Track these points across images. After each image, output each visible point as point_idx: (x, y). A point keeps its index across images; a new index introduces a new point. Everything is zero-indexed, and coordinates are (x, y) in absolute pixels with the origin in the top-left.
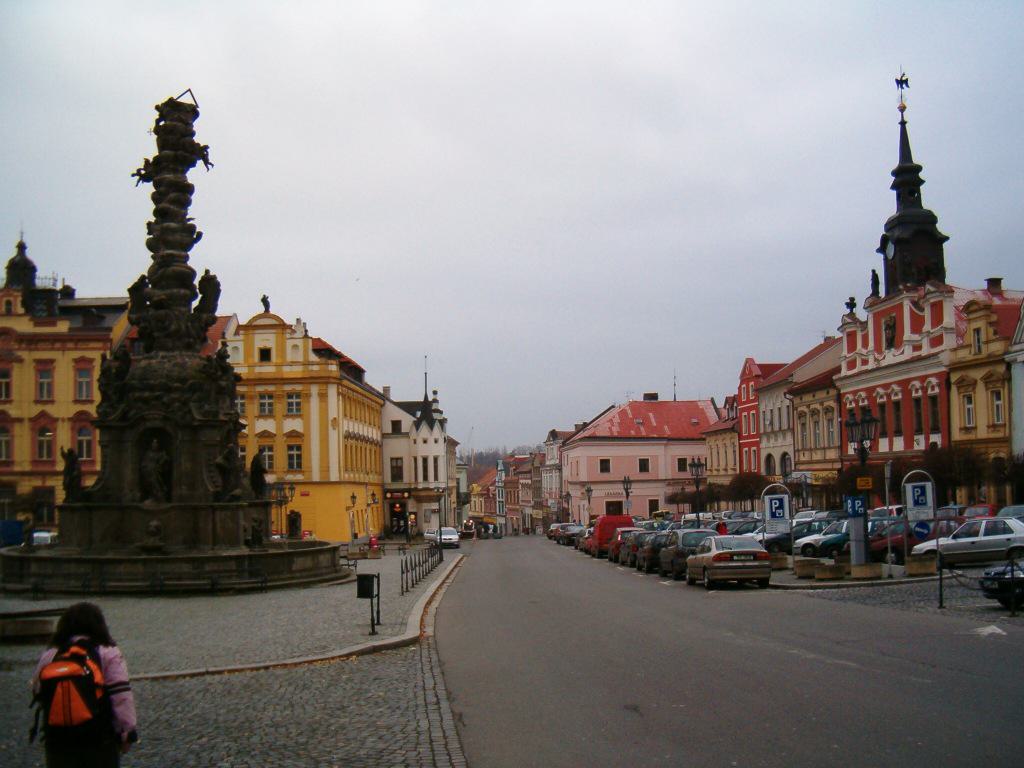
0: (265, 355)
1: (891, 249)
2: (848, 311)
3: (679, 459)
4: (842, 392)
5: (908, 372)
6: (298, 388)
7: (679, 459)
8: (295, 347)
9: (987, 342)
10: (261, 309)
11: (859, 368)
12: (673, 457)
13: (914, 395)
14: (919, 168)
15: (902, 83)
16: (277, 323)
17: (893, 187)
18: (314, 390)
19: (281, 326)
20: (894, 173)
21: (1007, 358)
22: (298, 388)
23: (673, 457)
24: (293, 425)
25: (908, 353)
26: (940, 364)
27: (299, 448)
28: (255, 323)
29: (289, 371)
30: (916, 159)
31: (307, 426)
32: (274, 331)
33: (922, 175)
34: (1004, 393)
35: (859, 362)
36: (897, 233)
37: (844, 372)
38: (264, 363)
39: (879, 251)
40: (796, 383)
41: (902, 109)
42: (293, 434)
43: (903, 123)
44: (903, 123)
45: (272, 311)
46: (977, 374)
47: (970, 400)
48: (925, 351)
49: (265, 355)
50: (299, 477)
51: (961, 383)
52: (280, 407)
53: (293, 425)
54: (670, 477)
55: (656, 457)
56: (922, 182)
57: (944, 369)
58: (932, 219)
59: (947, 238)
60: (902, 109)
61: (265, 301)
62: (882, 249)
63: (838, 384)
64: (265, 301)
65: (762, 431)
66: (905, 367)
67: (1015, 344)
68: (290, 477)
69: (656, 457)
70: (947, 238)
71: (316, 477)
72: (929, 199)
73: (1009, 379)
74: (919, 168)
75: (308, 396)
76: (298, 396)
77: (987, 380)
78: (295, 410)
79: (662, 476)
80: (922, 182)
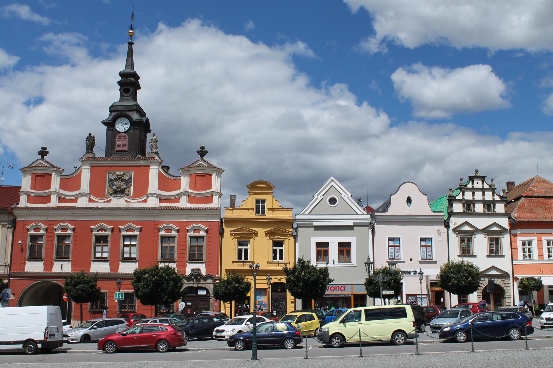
1: (122, 126)
2: (40, 157)
4: (19, 219)
5: (156, 216)
11: (54, 202)
20: (121, 74)
25: (153, 202)
35: (54, 198)
37: (23, 202)
39: (105, 123)
48: (183, 203)
62: (110, 124)
63: (16, 212)
66: (155, 212)
67: (303, 214)
73: (295, 238)
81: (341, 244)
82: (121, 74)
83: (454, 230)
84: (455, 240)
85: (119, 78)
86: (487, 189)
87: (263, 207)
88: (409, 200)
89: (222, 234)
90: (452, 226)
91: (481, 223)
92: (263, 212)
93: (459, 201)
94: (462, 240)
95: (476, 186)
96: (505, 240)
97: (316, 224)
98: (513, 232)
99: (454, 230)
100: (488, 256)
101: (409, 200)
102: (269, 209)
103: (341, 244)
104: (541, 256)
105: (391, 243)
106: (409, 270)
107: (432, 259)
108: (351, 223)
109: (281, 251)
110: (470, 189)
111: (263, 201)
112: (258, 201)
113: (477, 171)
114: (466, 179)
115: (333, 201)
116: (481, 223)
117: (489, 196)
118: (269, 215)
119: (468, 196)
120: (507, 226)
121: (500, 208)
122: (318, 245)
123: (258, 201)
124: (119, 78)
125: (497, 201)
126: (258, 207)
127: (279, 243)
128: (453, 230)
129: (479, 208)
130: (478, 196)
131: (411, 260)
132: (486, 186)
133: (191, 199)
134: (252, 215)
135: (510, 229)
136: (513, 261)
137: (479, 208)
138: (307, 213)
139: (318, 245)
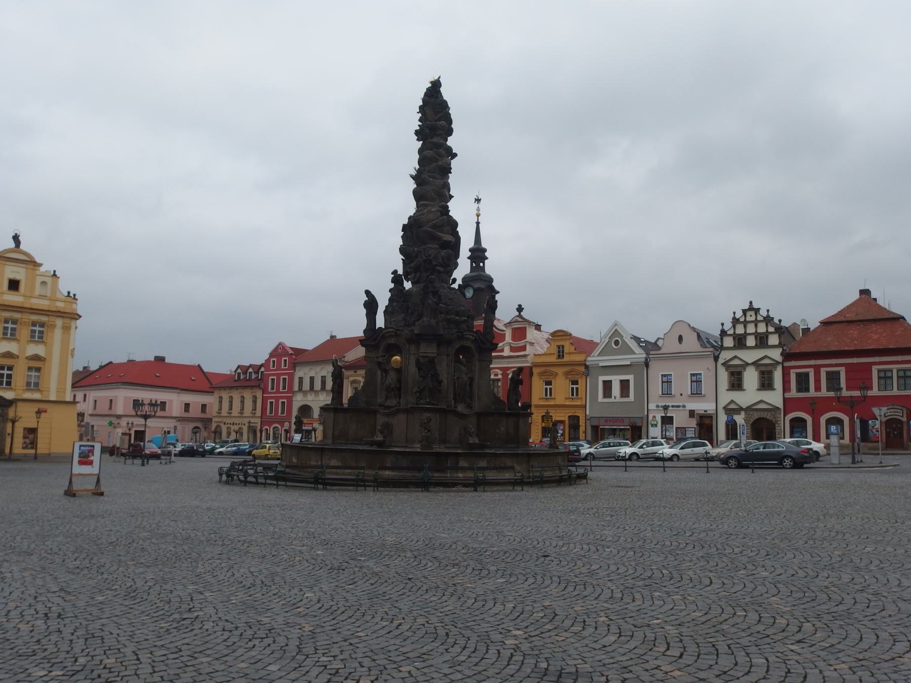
3: (185, 404)
6: (44, 319)
7: (185, 404)
9: (570, 353)
10: (12, 245)
13: (492, 377)
14: (485, 250)
15: (478, 200)
16: (28, 259)
17: (468, 258)
18: (59, 322)
19: (32, 263)
20: (471, 250)
21: (587, 363)
22: (44, 319)
24: (39, 350)
26: (527, 362)
27: (38, 370)
28: (7, 255)
29: (36, 303)
30: (484, 245)
31: (50, 352)
33: (486, 254)
34: (581, 382)
36: (477, 285)
38: (11, 292)
40: (346, 362)
41: (478, 215)
42: (36, 358)
43: (478, 223)
44: (478, 223)
45: (23, 247)
46: (560, 371)
47: (549, 383)
49: (14, 285)
50: (37, 396)
51: (541, 374)
52: (24, 333)
53: (39, 350)
54: (179, 416)
55: (171, 401)
56: (487, 258)
57: (529, 365)
58: (490, 280)
59: (498, 292)
60: (478, 215)
61: (16, 238)
64: (16, 238)
65: (296, 388)
67: (593, 356)
68: (28, 395)
69: (171, 401)
70: (498, 292)
71: (53, 398)
72: (490, 268)
74: (485, 250)
76: (42, 325)
77: (567, 374)
78: (39, 337)
79: (174, 415)
80: (487, 258)
81: (621, 381)
82: (471, 250)
83: (723, 364)
84: (723, 376)
85: (470, 253)
86: (761, 321)
87: (563, 352)
88: (680, 339)
89: (531, 374)
90: (721, 360)
91: (750, 356)
92: (563, 356)
93: (730, 335)
94: (732, 374)
95: (748, 319)
96: (778, 375)
97: (601, 364)
98: (787, 364)
99: (723, 364)
100: (758, 390)
101: (680, 339)
102: (566, 353)
103: (621, 381)
104: (818, 388)
105: (694, 378)
106: (678, 404)
107: (701, 394)
108: (628, 363)
109: (577, 389)
110: (741, 322)
111: (563, 347)
112: (559, 347)
113: (751, 303)
114: (739, 314)
115: (617, 343)
116: (750, 356)
117: (762, 328)
118: (567, 358)
119: (740, 330)
120: (780, 359)
121: (774, 340)
122: (605, 382)
123: (559, 347)
124: (469, 254)
125: (772, 333)
126: (559, 352)
127: (575, 382)
128: (722, 364)
129: (751, 341)
130: (751, 329)
131: (681, 395)
132: (760, 318)
133: (513, 349)
134: (553, 359)
135: (783, 361)
136: (785, 394)
137: (751, 341)
138: (596, 355)
139: (605, 382)
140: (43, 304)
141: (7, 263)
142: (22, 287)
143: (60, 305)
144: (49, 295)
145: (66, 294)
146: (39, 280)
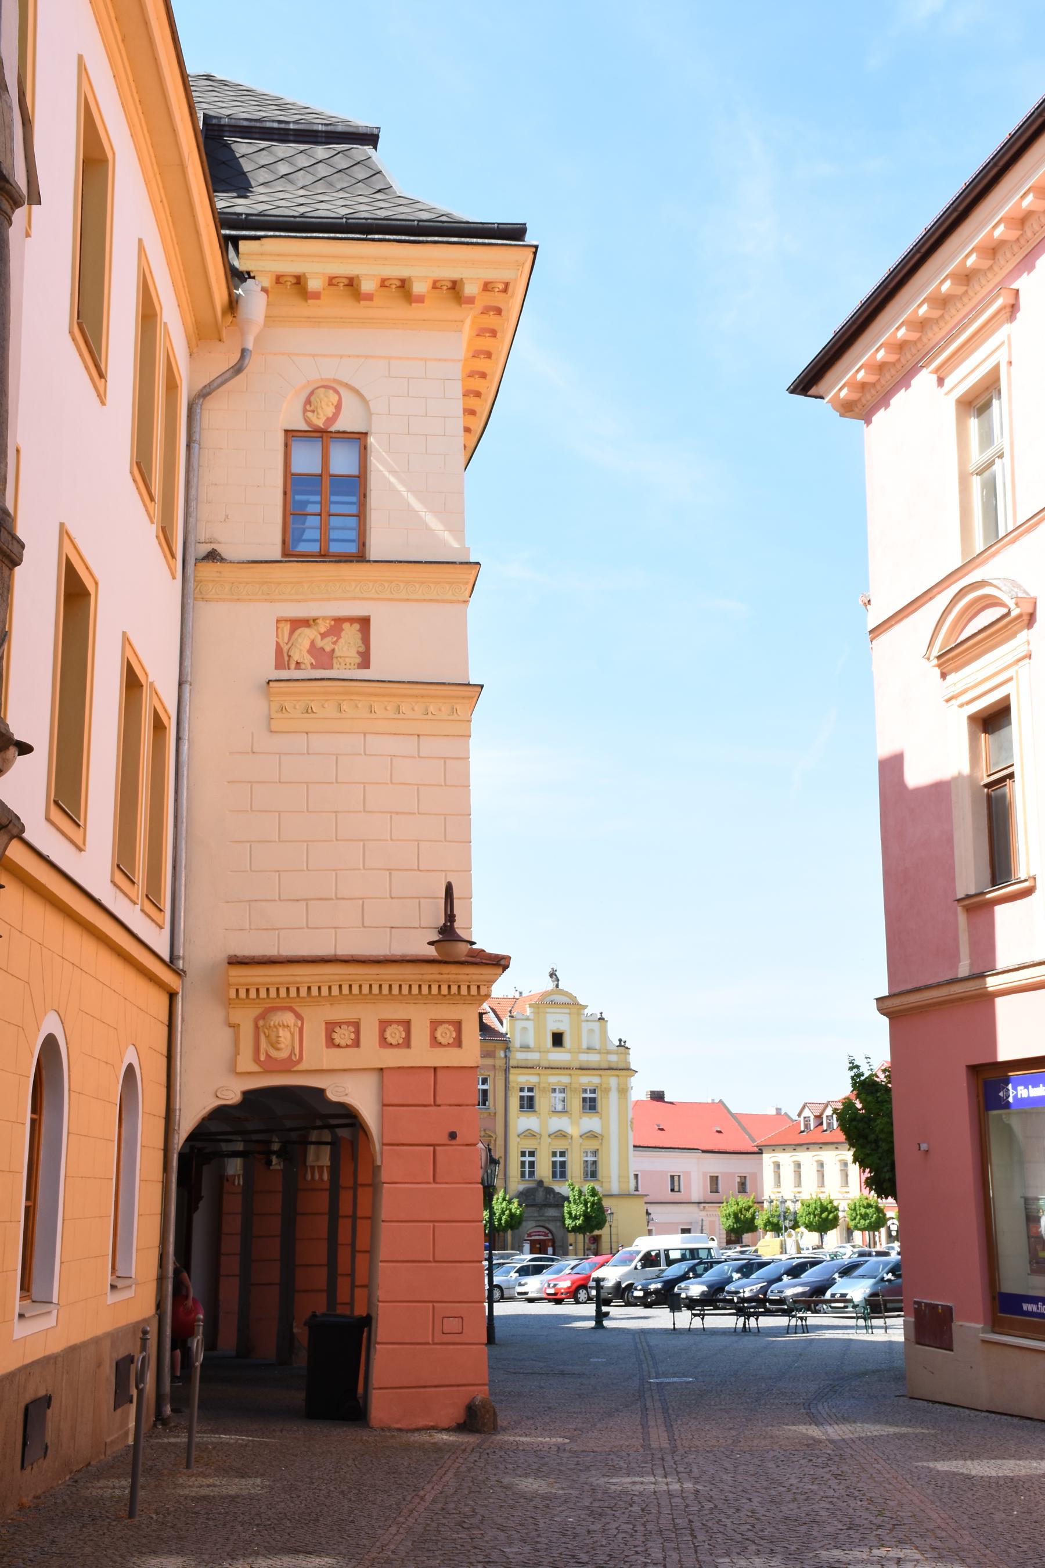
0: (558, 1039)
3: (711, 1177)
7: (711, 1177)
8: (592, 1031)
10: (550, 985)
12: (705, 1174)
18: (613, 1082)
19: (574, 1006)
23: (705, 1174)
32: (567, 1011)
42: (591, 1135)
49: (558, 1039)
61: (553, 974)
64: (553, 974)
69: (688, 1174)
75: (607, 1090)
79: (695, 1197)
140: (593, 1059)
141: (548, 1010)
142: (567, 1040)
143: (613, 1058)
144: (597, 1046)
145: (618, 1044)
146: (585, 1027)
